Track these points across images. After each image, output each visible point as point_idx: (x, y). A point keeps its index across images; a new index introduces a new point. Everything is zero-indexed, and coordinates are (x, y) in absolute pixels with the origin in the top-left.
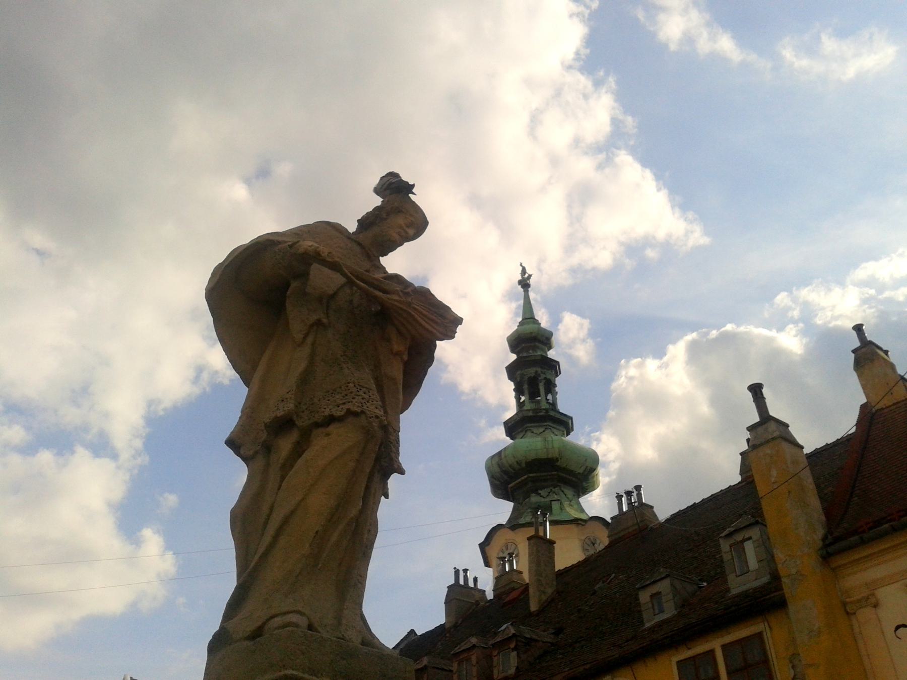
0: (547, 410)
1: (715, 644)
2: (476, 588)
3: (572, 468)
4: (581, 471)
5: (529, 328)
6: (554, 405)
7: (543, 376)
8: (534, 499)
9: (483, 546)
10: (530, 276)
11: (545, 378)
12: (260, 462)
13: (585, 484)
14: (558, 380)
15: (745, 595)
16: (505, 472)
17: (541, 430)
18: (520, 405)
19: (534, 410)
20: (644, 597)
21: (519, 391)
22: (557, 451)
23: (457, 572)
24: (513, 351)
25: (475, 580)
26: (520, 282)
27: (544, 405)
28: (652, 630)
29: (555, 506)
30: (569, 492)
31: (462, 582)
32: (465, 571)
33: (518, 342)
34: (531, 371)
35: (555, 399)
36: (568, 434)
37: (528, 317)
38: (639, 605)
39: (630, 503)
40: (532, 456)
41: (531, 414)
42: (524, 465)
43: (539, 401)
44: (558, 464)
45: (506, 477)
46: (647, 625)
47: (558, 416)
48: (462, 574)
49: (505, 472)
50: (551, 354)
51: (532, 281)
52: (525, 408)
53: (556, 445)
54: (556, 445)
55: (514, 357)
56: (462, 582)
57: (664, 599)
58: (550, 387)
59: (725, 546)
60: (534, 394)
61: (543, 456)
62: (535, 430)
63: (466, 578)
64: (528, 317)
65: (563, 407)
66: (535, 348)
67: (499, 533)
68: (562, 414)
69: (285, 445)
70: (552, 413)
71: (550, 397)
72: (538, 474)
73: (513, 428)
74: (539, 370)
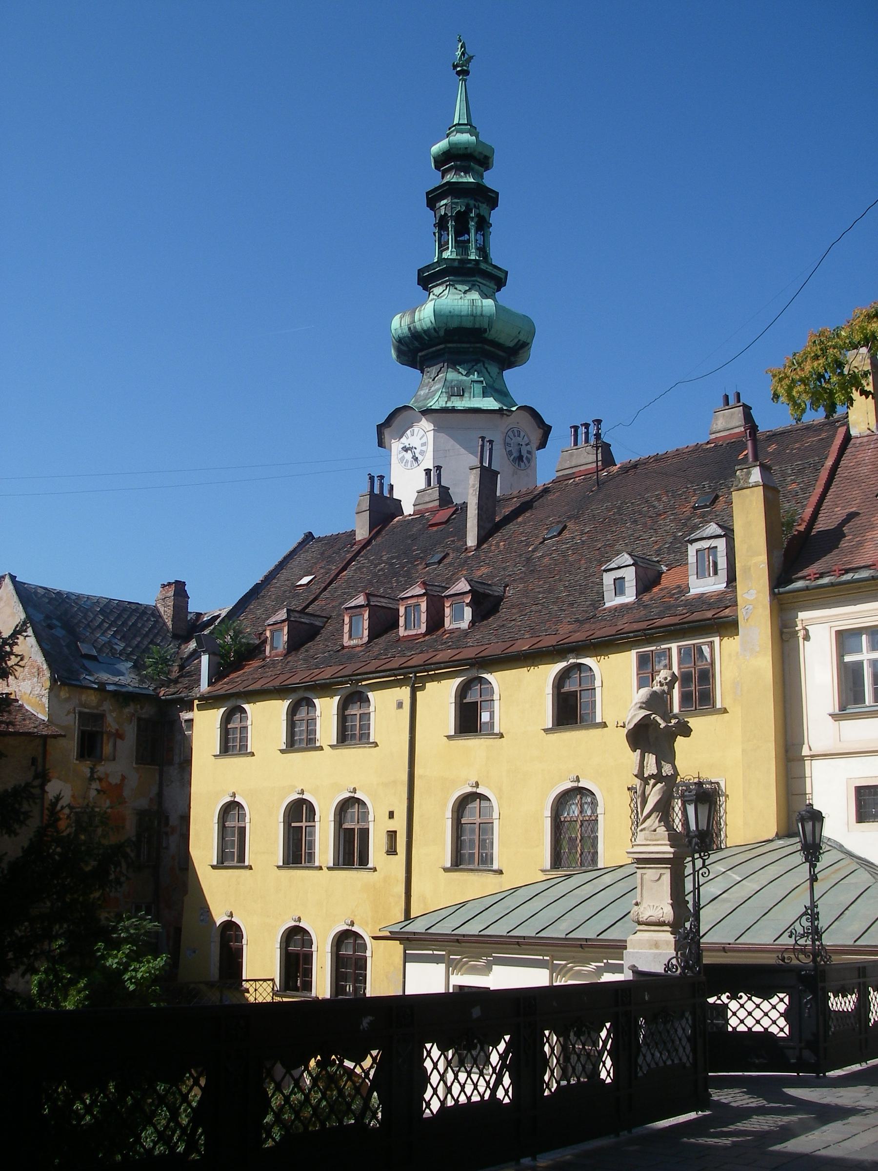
3: (501, 341)
4: (511, 345)
6: (483, 250)
8: (452, 375)
9: (381, 428)
13: (513, 359)
14: (495, 217)
18: (443, 247)
22: (486, 320)
23: (372, 478)
30: (494, 369)
31: (377, 491)
36: (498, 290)
40: (455, 324)
41: (456, 264)
42: (442, 333)
44: (486, 335)
45: (416, 344)
47: (490, 269)
50: (490, 179)
51: (472, 67)
56: (377, 491)
58: (483, 225)
61: (468, 324)
63: (382, 485)
65: (498, 257)
68: (495, 267)
70: (483, 266)
72: (459, 345)
74: (472, 202)
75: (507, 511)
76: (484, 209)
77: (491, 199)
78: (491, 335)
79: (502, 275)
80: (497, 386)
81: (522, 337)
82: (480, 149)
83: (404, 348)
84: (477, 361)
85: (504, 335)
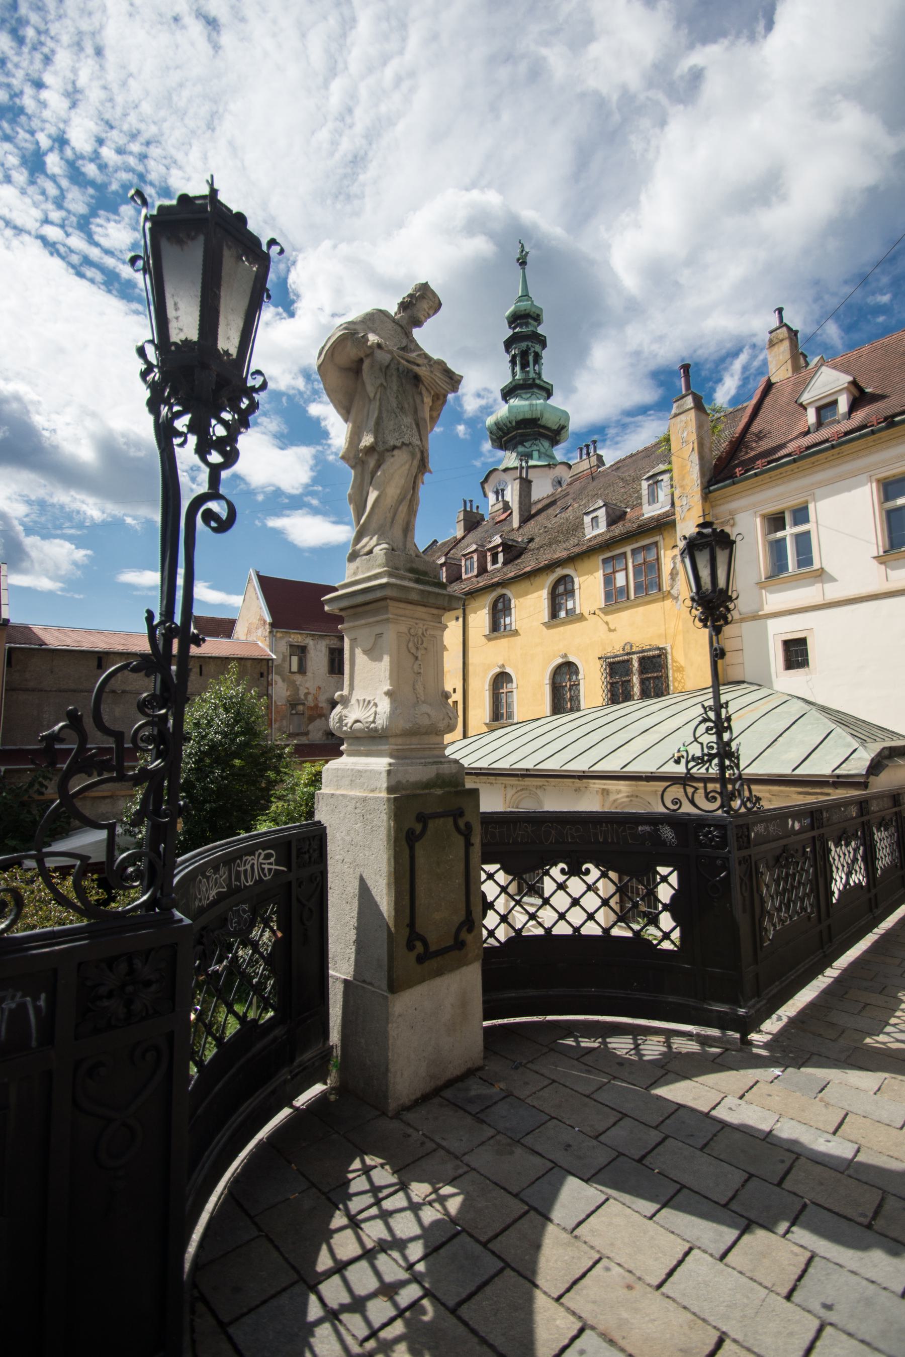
0: (534, 379)
1: (628, 549)
2: (477, 513)
3: (549, 426)
4: (556, 428)
5: (525, 304)
6: (539, 375)
7: (532, 349)
8: (520, 449)
9: (483, 483)
10: (527, 253)
11: (534, 352)
12: (359, 468)
14: (544, 354)
15: (652, 518)
16: (500, 429)
17: (529, 395)
18: (514, 374)
19: (524, 380)
20: (587, 519)
21: (513, 362)
22: (539, 412)
23: (465, 502)
24: (510, 327)
25: (478, 507)
26: (518, 260)
27: (532, 375)
28: (590, 540)
29: (536, 454)
30: (546, 444)
31: (468, 509)
32: (471, 501)
33: (516, 319)
34: (524, 345)
35: (540, 369)
36: (548, 398)
37: (526, 295)
38: (583, 524)
39: (588, 454)
40: (520, 417)
41: (521, 382)
42: (514, 424)
43: (528, 372)
46: (588, 537)
47: (542, 383)
48: (468, 505)
49: (500, 429)
50: (540, 330)
51: (528, 259)
52: (517, 377)
53: (539, 408)
54: (539, 408)
55: (510, 332)
56: (468, 509)
57: (600, 520)
58: (537, 358)
59: (645, 484)
60: (524, 366)
61: (528, 416)
62: (524, 396)
63: (471, 506)
64: (526, 295)
65: (547, 377)
66: (527, 324)
67: (496, 473)
69: (372, 463)
70: (537, 382)
71: (537, 367)
73: (508, 393)
74: (530, 344)
75: (540, 506)
76: (538, 348)
77: (543, 342)
78: (543, 422)
79: (550, 387)
80: (548, 453)
81: (562, 423)
82: (533, 310)
83: (494, 437)
84: (536, 439)
85: (550, 421)
